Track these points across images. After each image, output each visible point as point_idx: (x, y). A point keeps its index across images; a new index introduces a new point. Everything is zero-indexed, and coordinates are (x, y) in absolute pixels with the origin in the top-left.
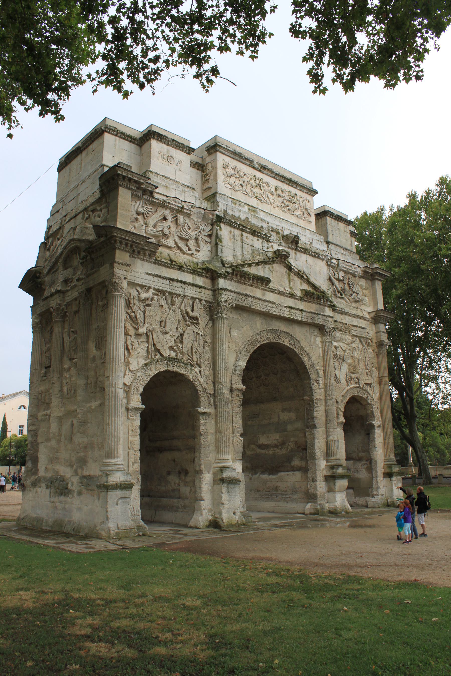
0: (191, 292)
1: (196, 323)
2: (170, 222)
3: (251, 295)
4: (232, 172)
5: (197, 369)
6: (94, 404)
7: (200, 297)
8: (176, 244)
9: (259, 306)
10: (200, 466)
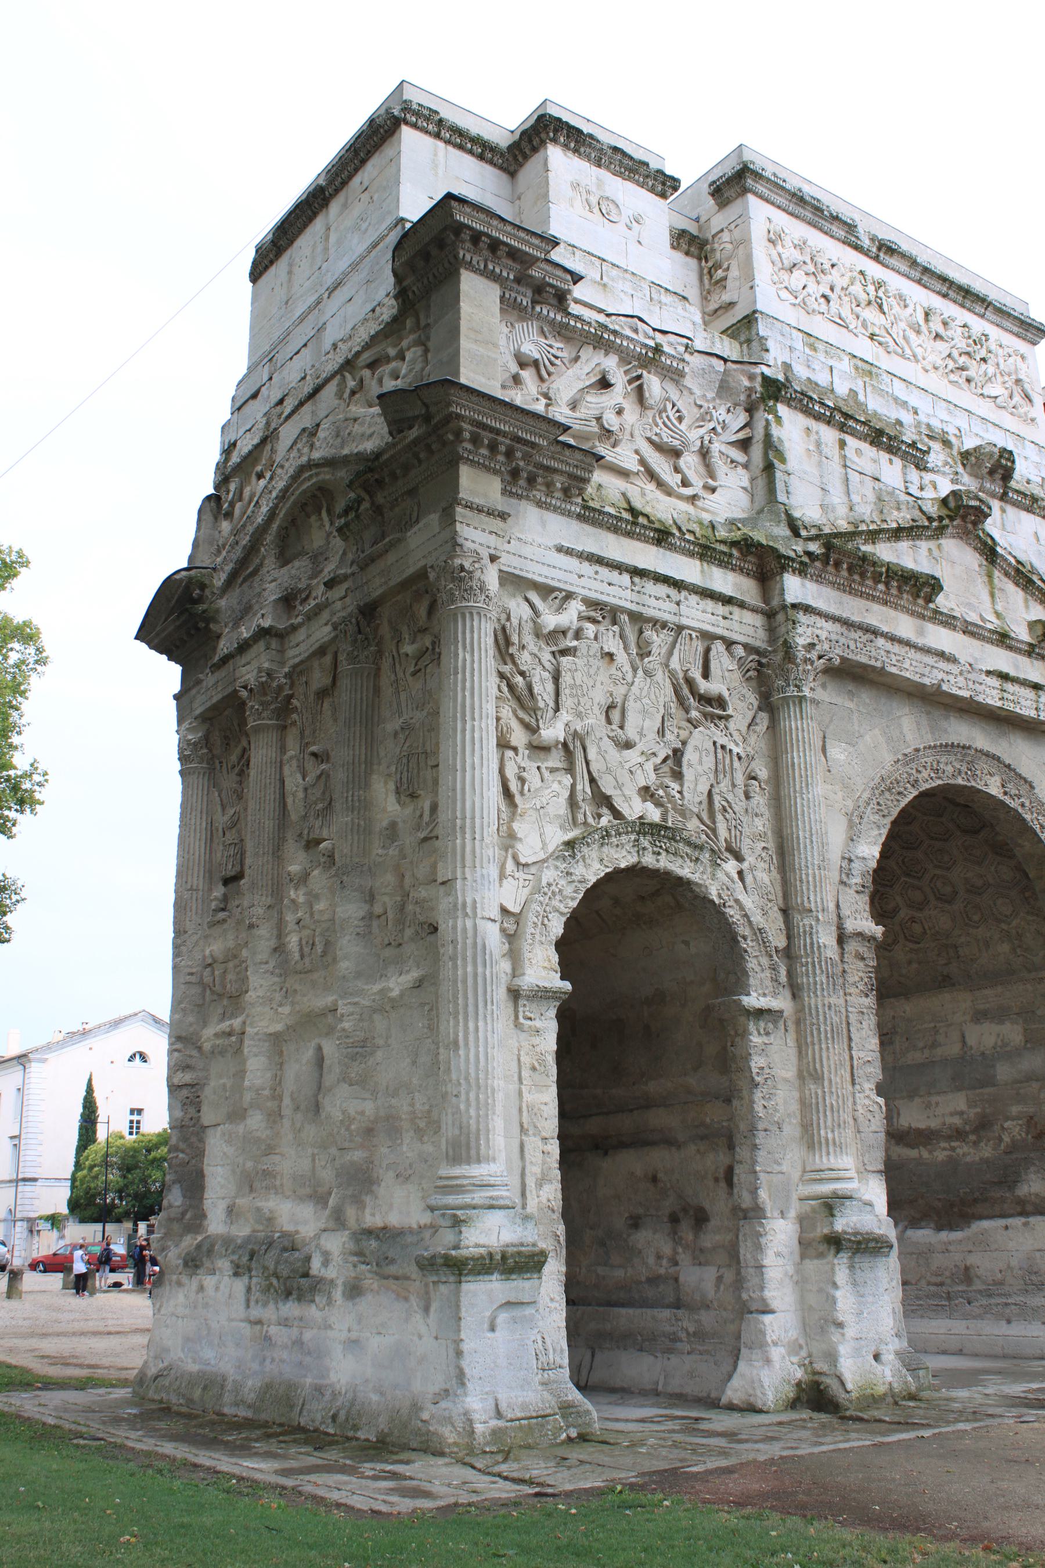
0: (698, 614)
1: (720, 718)
2: (620, 392)
3: (885, 629)
4: (796, 256)
5: (731, 866)
6: (397, 983)
7: (726, 634)
8: (642, 462)
9: (911, 667)
10: (754, 1191)
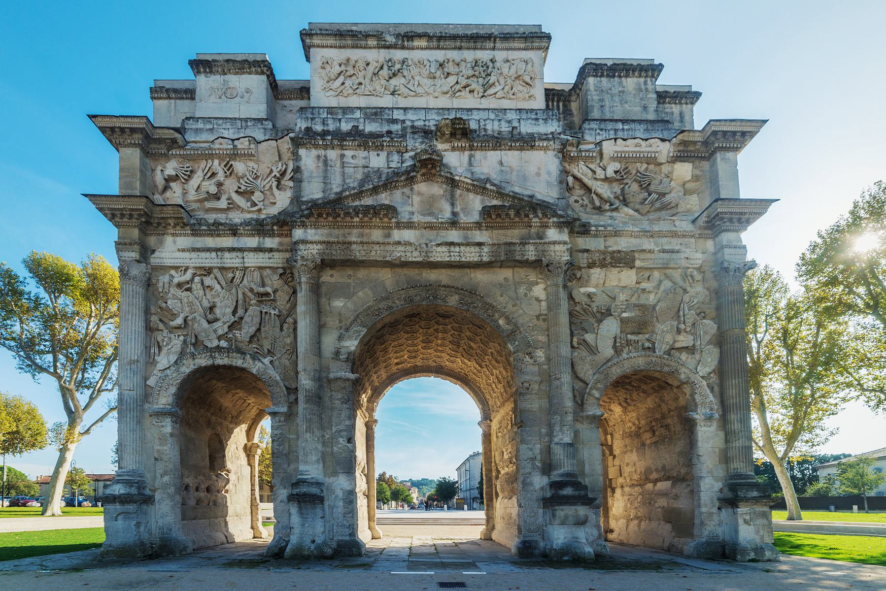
0: (253, 260)
